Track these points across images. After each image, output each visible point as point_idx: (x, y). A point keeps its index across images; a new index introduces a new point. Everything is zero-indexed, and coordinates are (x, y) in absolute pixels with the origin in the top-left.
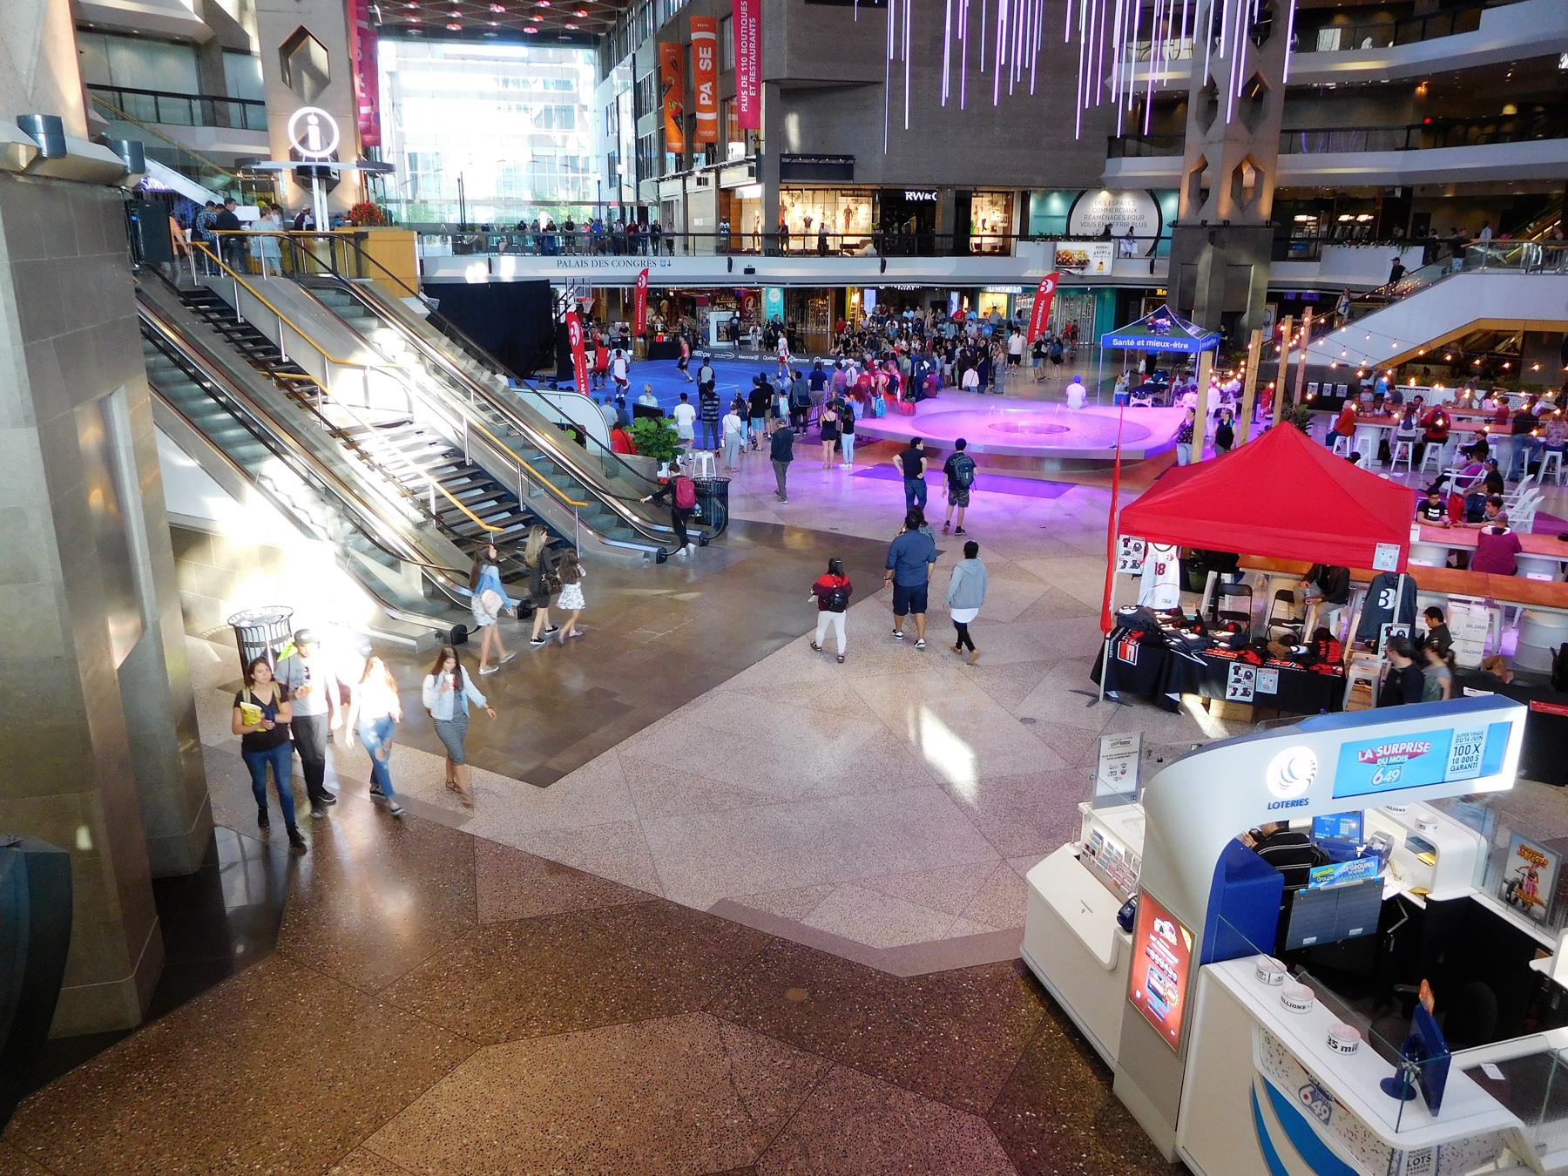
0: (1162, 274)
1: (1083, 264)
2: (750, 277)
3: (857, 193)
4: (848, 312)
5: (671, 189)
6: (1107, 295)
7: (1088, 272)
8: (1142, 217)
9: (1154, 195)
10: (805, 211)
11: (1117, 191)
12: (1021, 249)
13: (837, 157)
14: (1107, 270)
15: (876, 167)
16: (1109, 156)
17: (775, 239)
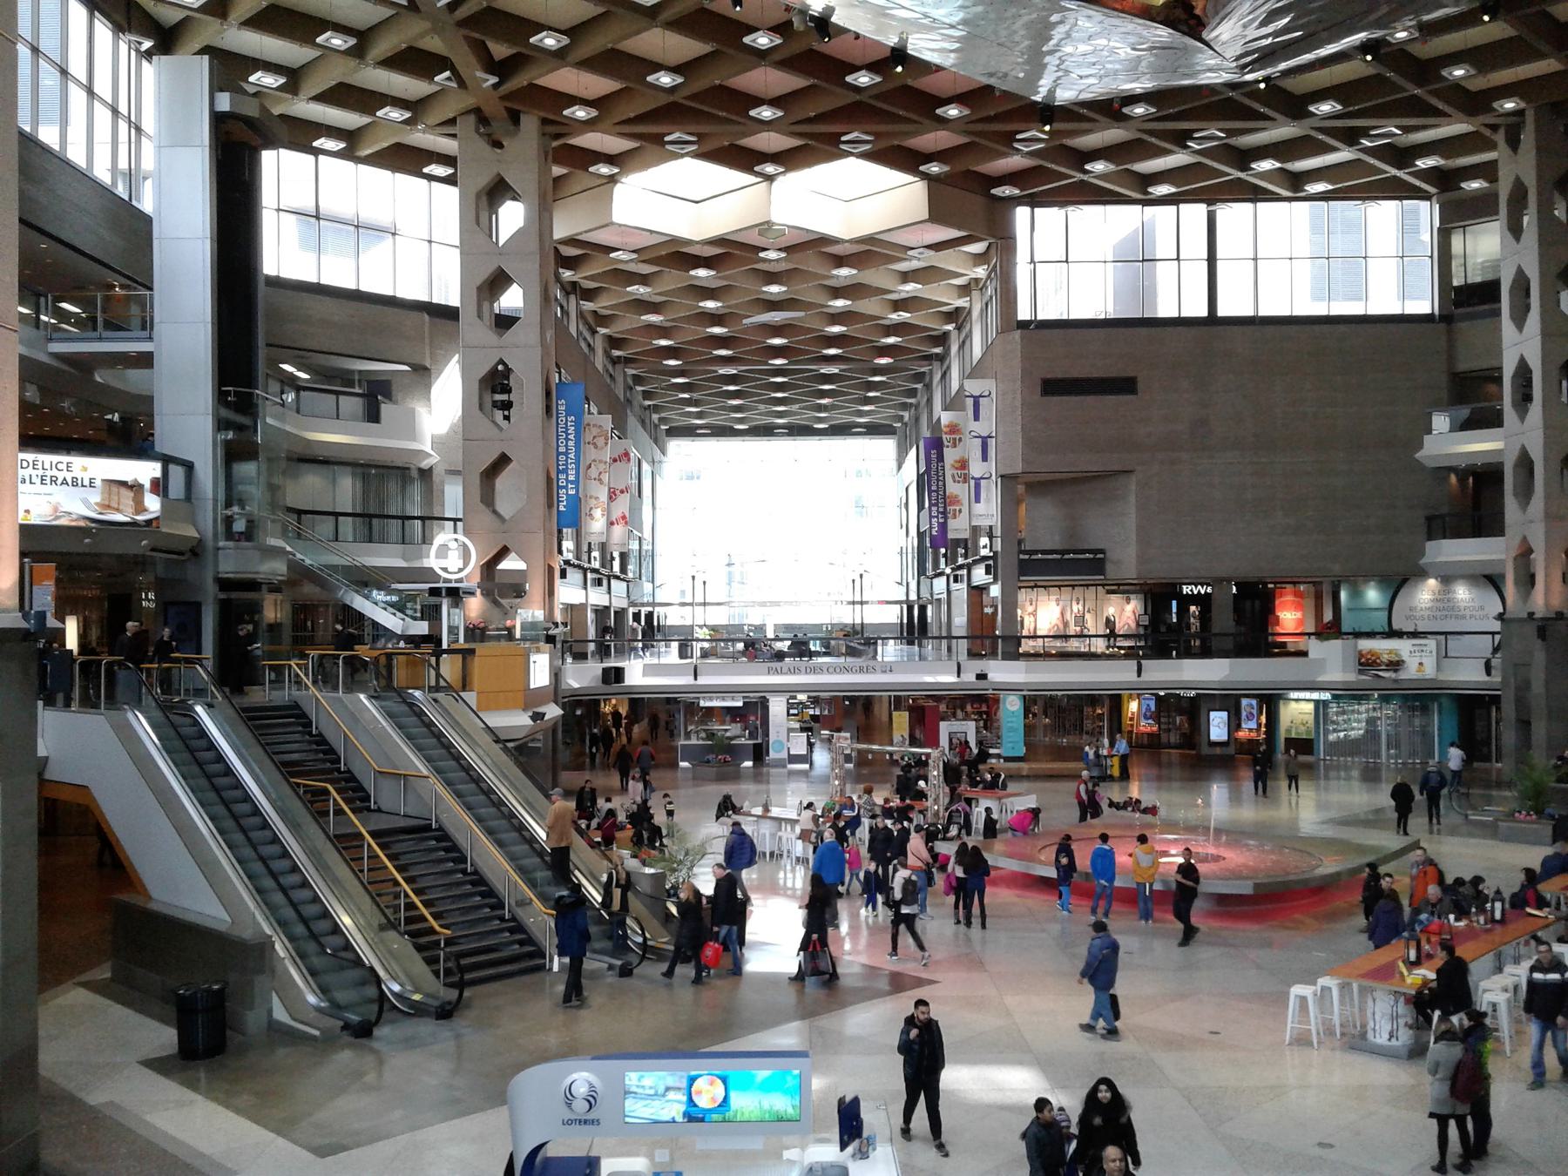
0: (1497, 678)
1: (1396, 665)
2: (982, 684)
3: (1121, 588)
4: (1126, 722)
5: (940, 584)
6: (1445, 702)
7: (1403, 675)
8: (1482, 608)
9: (1494, 581)
10: (1044, 613)
11: (1447, 580)
12: (1315, 648)
14: (1430, 671)
15: (1126, 560)
16: (1430, 539)
17: (1010, 645)
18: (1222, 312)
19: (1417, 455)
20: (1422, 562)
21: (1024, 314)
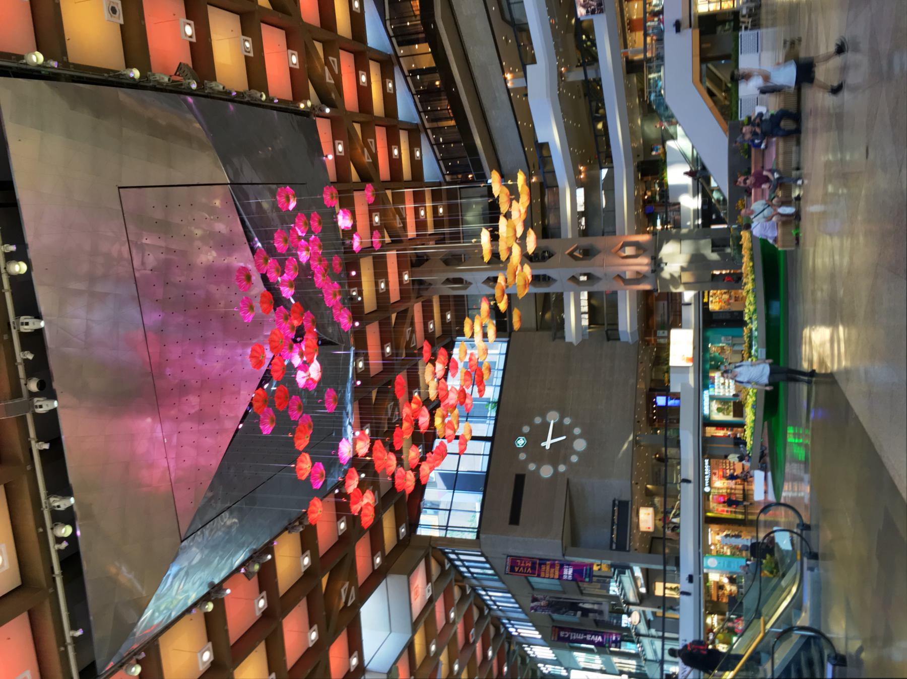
2: (696, 579)
13: (613, 511)
16: (619, 339)
18: (490, 434)
19: (575, 343)
20: (630, 341)
21: (472, 536)
